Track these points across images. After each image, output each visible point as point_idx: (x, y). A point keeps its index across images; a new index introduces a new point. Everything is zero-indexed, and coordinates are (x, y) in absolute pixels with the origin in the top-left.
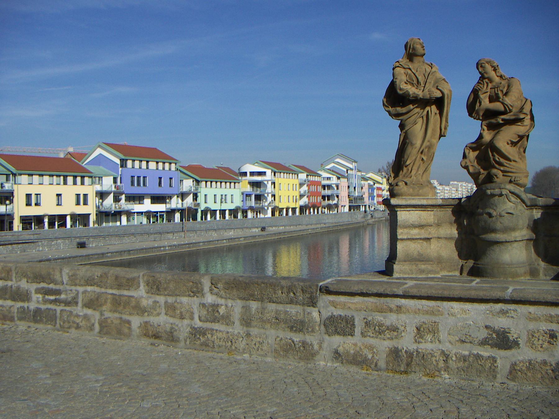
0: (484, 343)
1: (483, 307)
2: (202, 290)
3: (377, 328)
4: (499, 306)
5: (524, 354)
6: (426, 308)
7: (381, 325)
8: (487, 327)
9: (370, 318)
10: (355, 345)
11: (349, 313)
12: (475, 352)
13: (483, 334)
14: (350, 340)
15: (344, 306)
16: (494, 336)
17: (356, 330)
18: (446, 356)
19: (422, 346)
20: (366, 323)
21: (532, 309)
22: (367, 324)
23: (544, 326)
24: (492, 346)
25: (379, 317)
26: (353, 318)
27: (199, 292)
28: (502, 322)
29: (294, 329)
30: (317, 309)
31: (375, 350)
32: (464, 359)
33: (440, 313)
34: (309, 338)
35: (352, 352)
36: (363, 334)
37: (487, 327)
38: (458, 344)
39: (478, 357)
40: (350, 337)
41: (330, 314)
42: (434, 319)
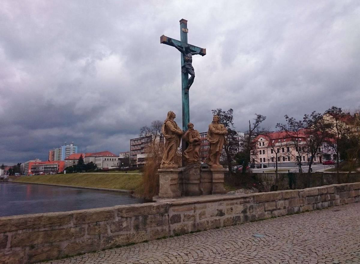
0: (217, 215)
1: (217, 203)
2: (114, 215)
3: (188, 217)
4: (220, 202)
5: (227, 216)
6: (202, 207)
7: (189, 216)
8: (217, 210)
9: (186, 214)
10: (181, 225)
11: (179, 213)
12: (215, 219)
13: (216, 212)
14: (179, 224)
15: (177, 210)
16: (219, 212)
17: (181, 219)
18: (208, 222)
19: (201, 221)
20: (185, 216)
21: (227, 202)
22: (185, 216)
23: (229, 207)
24: (219, 216)
25: (188, 213)
26: (180, 215)
27: (111, 217)
28: (220, 208)
29: (159, 225)
30: (167, 214)
31: (188, 226)
32: (212, 222)
33: (206, 208)
34: (164, 227)
35: (180, 229)
36: (184, 221)
37: (217, 210)
38: (211, 217)
39: (216, 220)
40: (179, 223)
41: (172, 215)
42: (204, 210)
